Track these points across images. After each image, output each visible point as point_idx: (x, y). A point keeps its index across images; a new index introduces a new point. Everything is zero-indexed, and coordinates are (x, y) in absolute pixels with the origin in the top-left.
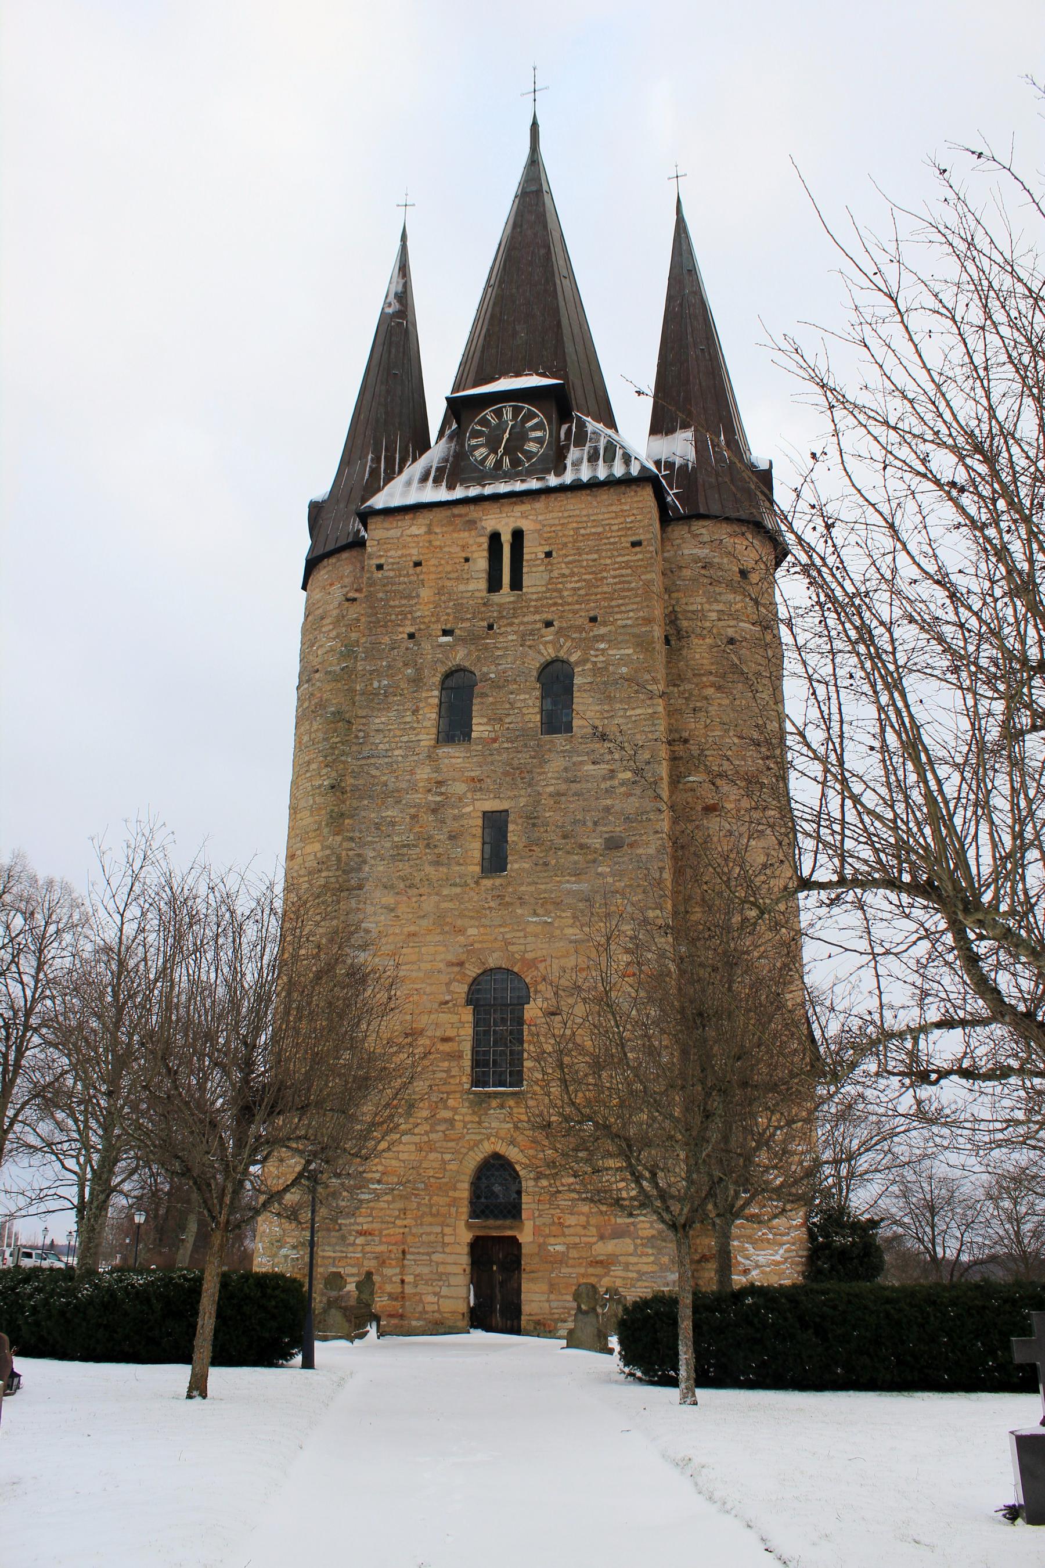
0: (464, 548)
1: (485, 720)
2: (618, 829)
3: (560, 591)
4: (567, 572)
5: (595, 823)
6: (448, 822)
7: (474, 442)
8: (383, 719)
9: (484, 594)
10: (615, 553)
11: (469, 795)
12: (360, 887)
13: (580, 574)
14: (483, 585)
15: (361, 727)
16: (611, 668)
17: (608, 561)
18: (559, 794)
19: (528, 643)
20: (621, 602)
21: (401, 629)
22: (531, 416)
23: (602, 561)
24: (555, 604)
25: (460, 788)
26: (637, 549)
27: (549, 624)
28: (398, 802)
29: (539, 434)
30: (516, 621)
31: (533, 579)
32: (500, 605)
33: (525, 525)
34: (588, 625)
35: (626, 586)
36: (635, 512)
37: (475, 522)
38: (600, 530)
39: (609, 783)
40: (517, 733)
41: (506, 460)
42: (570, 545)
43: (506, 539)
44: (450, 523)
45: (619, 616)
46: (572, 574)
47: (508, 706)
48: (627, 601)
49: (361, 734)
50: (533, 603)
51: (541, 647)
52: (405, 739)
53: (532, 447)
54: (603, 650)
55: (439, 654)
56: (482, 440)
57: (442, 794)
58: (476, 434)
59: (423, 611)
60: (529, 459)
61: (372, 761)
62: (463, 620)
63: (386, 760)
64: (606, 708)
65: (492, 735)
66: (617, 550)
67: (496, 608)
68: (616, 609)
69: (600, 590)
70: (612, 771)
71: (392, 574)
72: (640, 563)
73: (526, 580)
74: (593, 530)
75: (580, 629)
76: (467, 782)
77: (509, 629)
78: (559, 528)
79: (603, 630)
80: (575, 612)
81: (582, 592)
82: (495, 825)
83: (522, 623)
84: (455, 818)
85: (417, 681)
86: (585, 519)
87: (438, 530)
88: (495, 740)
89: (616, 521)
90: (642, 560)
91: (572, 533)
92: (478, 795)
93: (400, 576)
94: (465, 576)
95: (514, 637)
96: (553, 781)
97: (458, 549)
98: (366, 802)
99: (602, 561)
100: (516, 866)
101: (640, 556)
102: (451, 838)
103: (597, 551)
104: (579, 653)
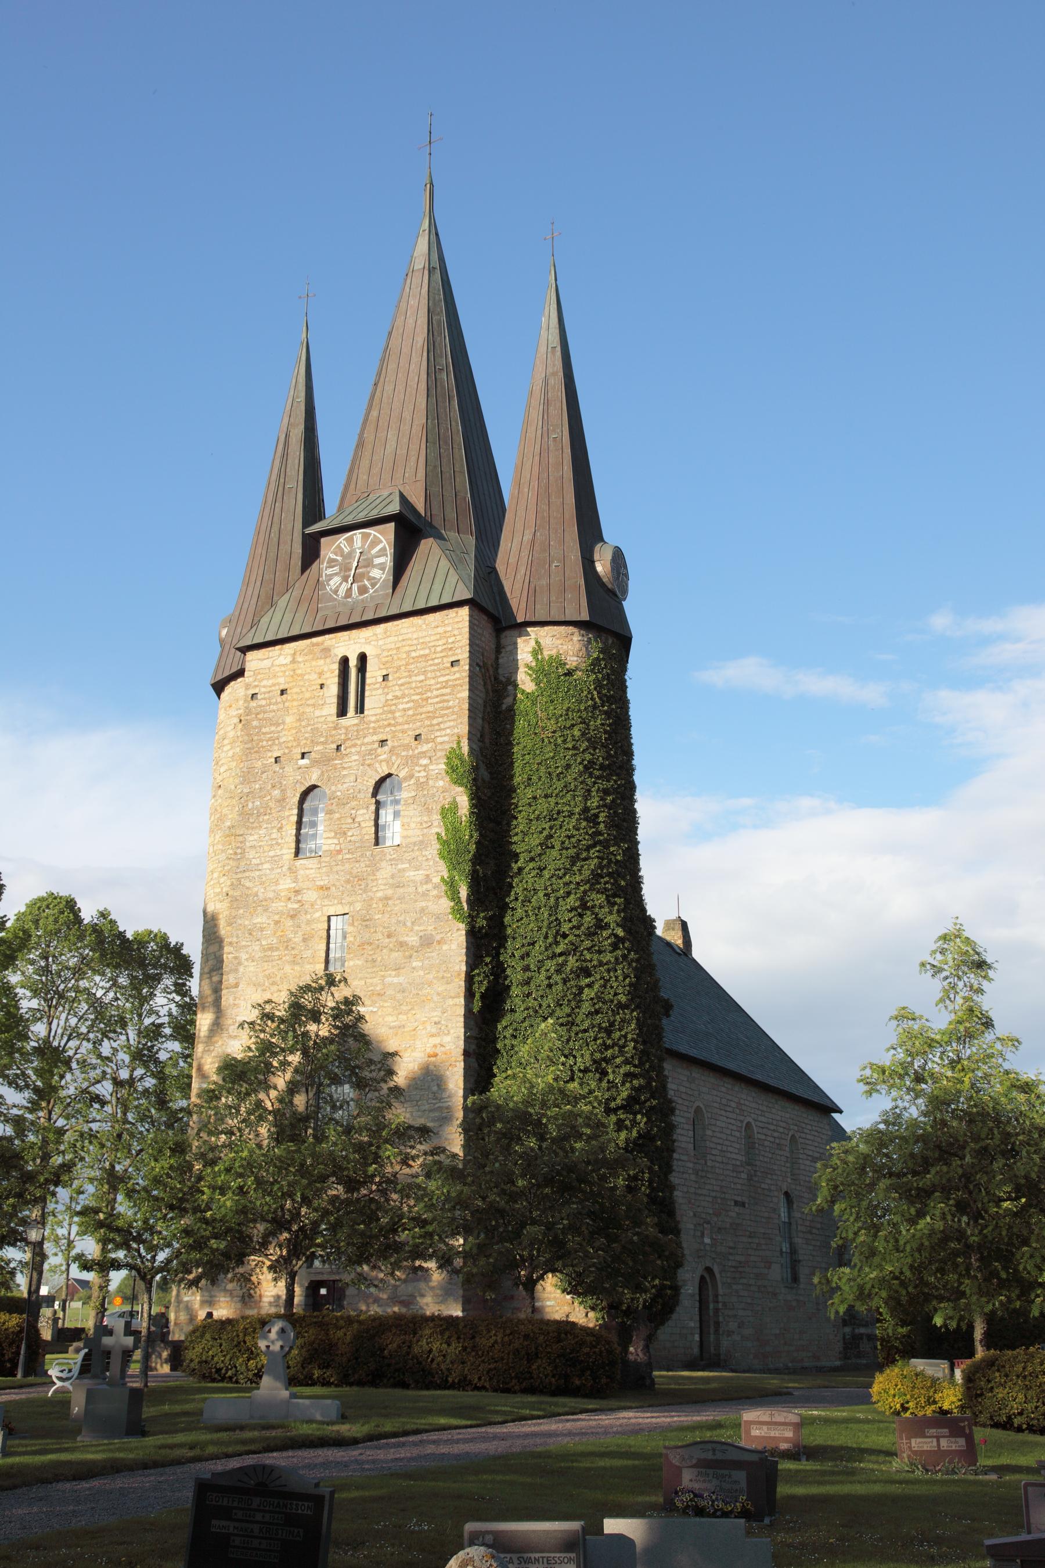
0: (321, 674)
1: (333, 834)
2: (430, 928)
3: (392, 712)
4: (399, 694)
5: (413, 923)
6: (303, 926)
7: (329, 571)
8: (256, 837)
9: (335, 718)
10: (438, 674)
11: (319, 902)
12: (236, 986)
13: (410, 695)
14: (333, 709)
15: (239, 845)
16: (431, 782)
17: (432, 682)
18: (387, 898)
19: (367, 762)
20: (440, 720)
21: (270, 754)
22: (376, 542)
23: (428, 682)
24: (389, 725)
25: (311, 896)
26: (456, 669)
28: (266, 910)
29: (382, 560)
30: (359, 742)
32: (347, 728)
34: (414, 743)
35: (446, 704)
36: (456, 632)
37: (330, 650)
38: (427, 651)
39: (425, 887)
40: (357, 845)
41: (355, 587)
42: (403, 668)
43: (353, 663)
44: (311, 652)
45: (438, 734)
46: (403, 696)
47: (350, 821)
48: (445, 719)
49: (239, 851)
50: (372, 725)
51: (377, 765)
52: (272, 853)
53: (376, 573)
54: (425, 766)
56: (336, 569)
57: (299, 901)
58: (332, 563)
59: (286, 737)
60: (373, 585)
61: (247, 874)
62: (318, 743)
63: (257, 873)
64: (425, 819)
65: (338, 848)
66: (439, 670)
67: (343, 731)
68: (437, 727)
69: (424, 710)
70: (427, 876)
71: (263, 702)
72: (458, 682)
74: (422, 653)
75: (407, 747)
77: (353, 750)
78: (395, 652)
80: (403, 732)
81: (411, 712)
83: (363, 744)
84: (308, 923)
85: (282, 800)
86: (415, 642)
87: (300, 659)
89: (440, 643)
90: (459, 679)
91: (405, 656)
92: (326, 902)
93: (270, 705)
94: (321, 702)
95: (356, 757)
96: (382, 887)
97: (315, 676)
98: (241, 911)
99: (428, 682)
100: (351, 963)
101: (457, 675)
102: (304, 940)
103: (425, 673)
104: (406, 770)
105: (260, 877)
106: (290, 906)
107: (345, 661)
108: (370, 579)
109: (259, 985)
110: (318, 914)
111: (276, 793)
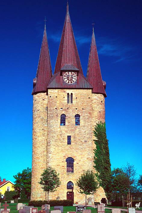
7: (65, 77)
25: (64, 132)
27: (76, 109)
29: (75, 78)
31: (74, 102)
33: (73, 93)
43: (70, 94)
46: (80, 102)
55: (60, 112)
73: (73, 102)
76: (65, 131)
79: (84, 111)
80: (80, 108)
82: (69, 138)
85: (57, 116)
88: (69, 126)
92: (67, 133)
105: (53, 128)
106: (60, 133)
107: (68, 94)
108: (72, 80)
109: (55, 146)
110: (65, 135)
111: (56, 114)
